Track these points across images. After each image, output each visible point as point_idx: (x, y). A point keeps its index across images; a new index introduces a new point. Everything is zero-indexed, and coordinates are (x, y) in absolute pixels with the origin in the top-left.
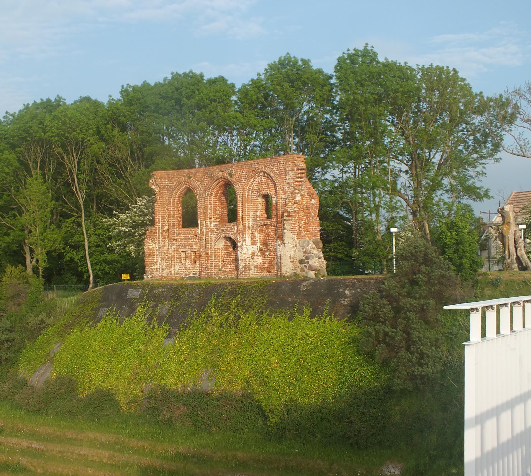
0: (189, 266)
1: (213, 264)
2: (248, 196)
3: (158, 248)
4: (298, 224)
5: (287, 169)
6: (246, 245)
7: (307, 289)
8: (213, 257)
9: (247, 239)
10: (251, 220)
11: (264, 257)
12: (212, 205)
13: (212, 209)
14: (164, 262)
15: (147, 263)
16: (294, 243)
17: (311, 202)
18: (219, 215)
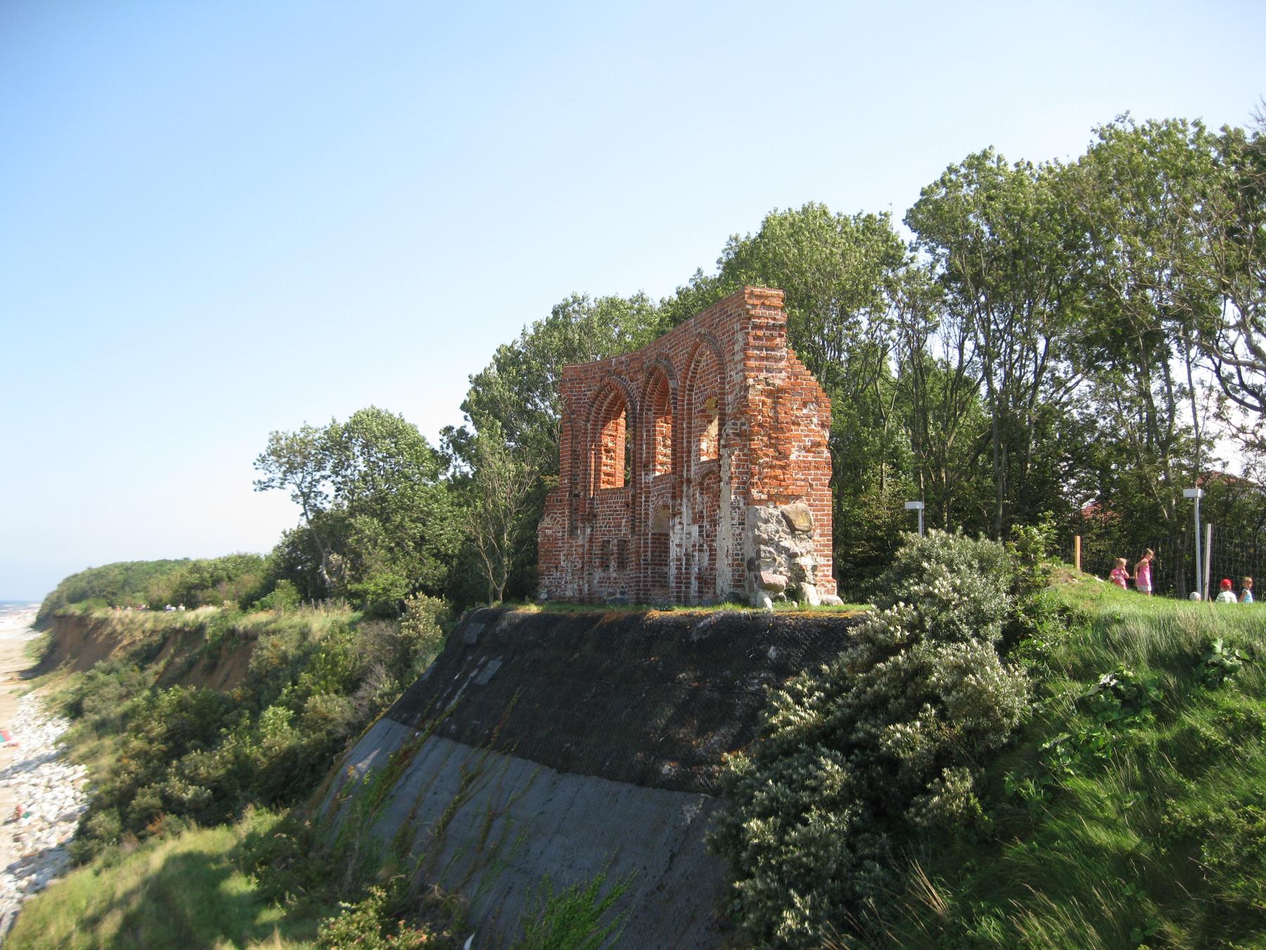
0: (614, 575)
2: (688, 404)
3: (560, 534)
6: (680, 523)
7: (701, 639)
8: (649, 554)
9: (684, 509)
11: (711, 550)
15: (542, 566)
16: (736, 516)
17: (805, 411)
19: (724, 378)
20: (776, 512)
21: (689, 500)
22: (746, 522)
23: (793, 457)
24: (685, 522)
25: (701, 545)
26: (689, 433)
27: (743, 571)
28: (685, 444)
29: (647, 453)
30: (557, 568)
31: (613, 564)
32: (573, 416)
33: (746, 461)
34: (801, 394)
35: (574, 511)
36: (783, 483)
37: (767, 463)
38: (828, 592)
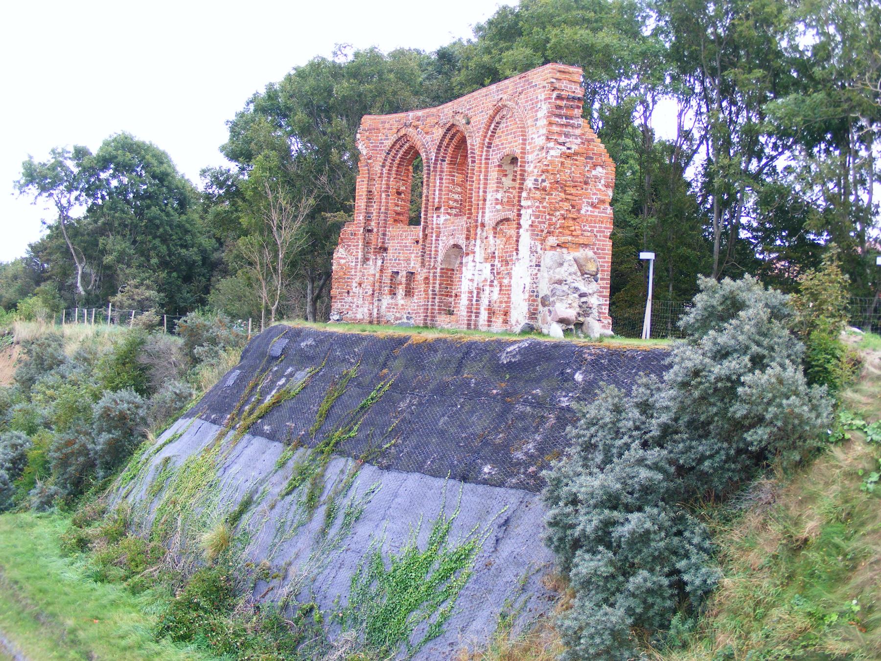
0: (401, 302)
1: (437, 300)
2: (486, 159)
3: (354, 264)
4: (548, 217)
5: (540, 98)
6: (474, 261)
7: (510, 361)
8: (437, 286)
9: (477, 249)
10: (487, 211)
12: (444, 181)
13: (443, 189)
14: (361, 291)
16: (534, 259)
17: (594, 173)
18: (456, 201)
19: (525, 140)
20: (570, 257)
21: (482, 242)
22: (542, 264)
23: (583, 212)
24: (477, 259)
25: (492, 281)
26: (485, 184)
27: (537, 305)
28: (481, 194)
29: (440, 198)
30: (348, 292)
31: (401, 291)
32: (369, 161)
33: (544, 212)
34: (591, 158)
35: (367, 244)
36: (574, 233)
37: (562, 215)
38: (604, 327)
